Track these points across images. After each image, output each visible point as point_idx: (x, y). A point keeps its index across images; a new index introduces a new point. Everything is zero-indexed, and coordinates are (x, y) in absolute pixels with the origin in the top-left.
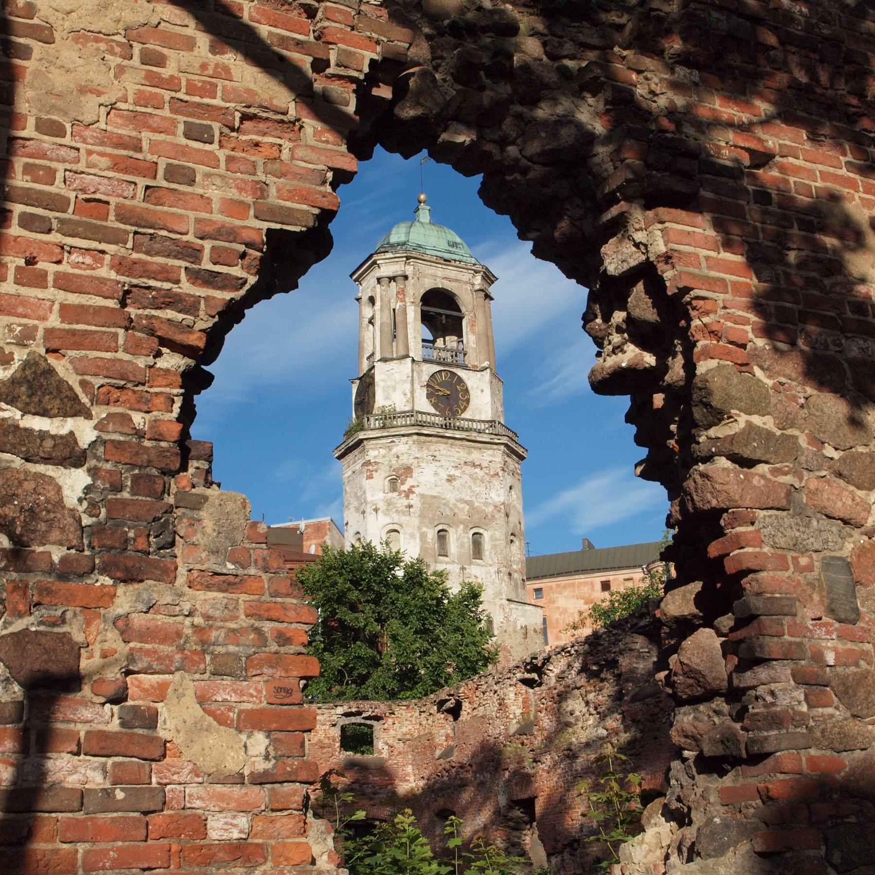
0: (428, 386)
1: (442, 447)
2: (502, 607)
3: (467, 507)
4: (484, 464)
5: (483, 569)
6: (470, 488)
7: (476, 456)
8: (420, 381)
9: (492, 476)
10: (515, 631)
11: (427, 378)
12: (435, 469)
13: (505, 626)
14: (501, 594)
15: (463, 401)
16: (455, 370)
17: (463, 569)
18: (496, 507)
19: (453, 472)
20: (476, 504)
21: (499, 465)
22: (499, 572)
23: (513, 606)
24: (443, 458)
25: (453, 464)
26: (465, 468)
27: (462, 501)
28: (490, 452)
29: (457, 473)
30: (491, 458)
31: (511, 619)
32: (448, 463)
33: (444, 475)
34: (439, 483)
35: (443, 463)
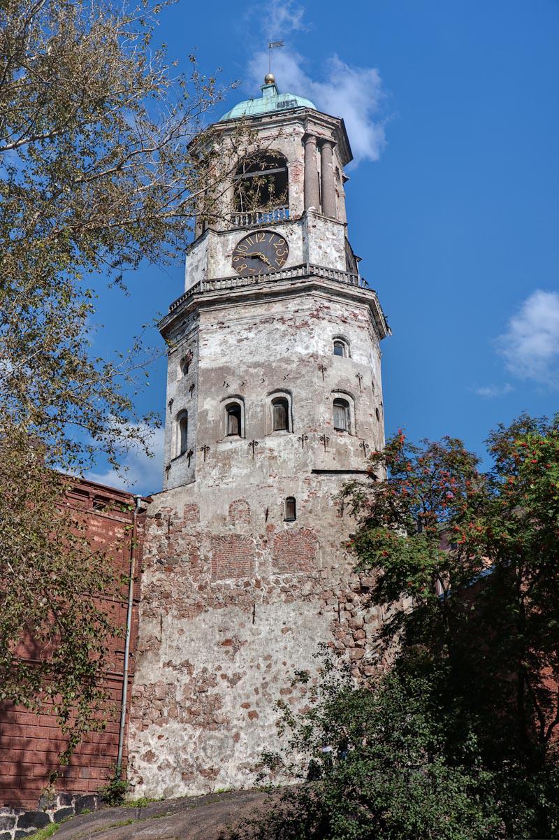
0: (235, 254)
1: (232, 311)
2: (307, 481)
3: (261, 371)
4: (286, 316)
5: (281, 440)
6: (268, 348)
7: (277, 308)
8: (225, 251)
9: (298, 328)
10: (324, 509)
11: (234, 246)
12: (222, 337)
13: (309, 506)
14: (305, 465)
15: (280, 258)
16: (270, 229)
17: (253, 444)
18: (301, 360)
19: (245, 334)
20: (274, 365)
21: (308, 313)
22: (303, 439)
23: (323, 477)
24: (231, 324)
25: (246, 326)
26: (261, 327)
27: (256, 365)
28: (297, 301)
29: (251, 335)
30: (293, 309)
31: (320, 494)
32: (239, 327)
33: (232, 340)
34: (228, 352)
35: (233, 328)
